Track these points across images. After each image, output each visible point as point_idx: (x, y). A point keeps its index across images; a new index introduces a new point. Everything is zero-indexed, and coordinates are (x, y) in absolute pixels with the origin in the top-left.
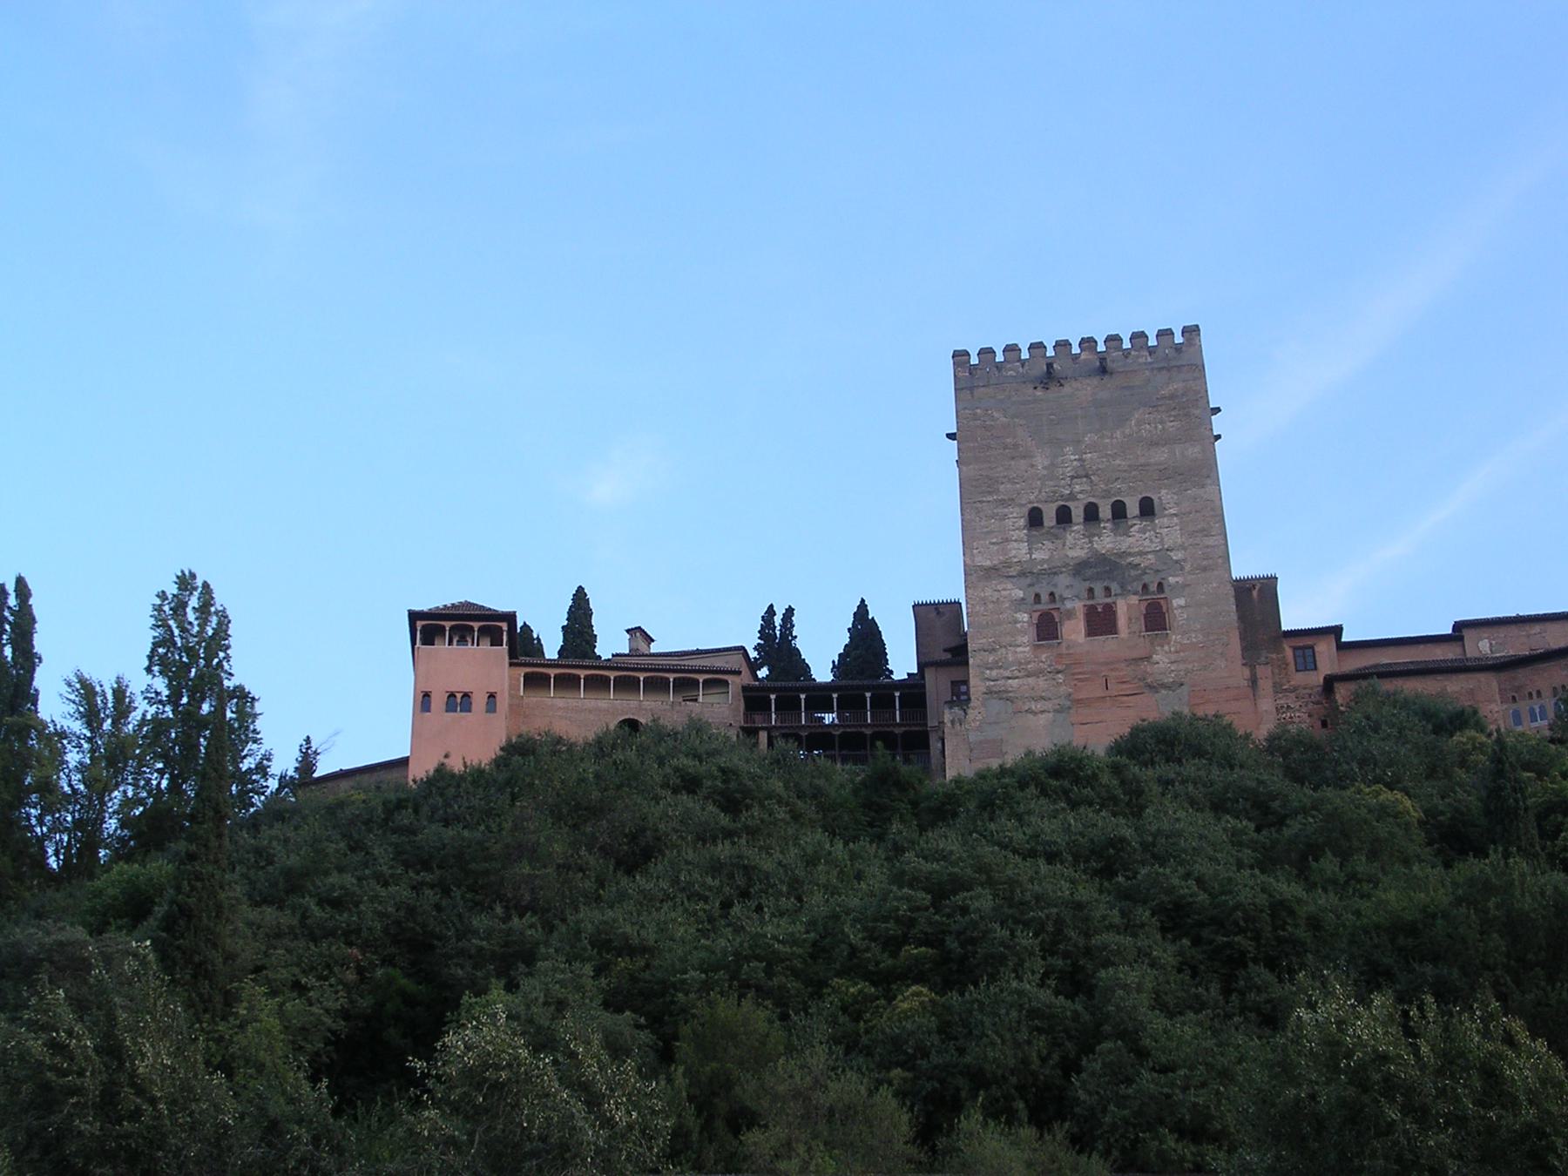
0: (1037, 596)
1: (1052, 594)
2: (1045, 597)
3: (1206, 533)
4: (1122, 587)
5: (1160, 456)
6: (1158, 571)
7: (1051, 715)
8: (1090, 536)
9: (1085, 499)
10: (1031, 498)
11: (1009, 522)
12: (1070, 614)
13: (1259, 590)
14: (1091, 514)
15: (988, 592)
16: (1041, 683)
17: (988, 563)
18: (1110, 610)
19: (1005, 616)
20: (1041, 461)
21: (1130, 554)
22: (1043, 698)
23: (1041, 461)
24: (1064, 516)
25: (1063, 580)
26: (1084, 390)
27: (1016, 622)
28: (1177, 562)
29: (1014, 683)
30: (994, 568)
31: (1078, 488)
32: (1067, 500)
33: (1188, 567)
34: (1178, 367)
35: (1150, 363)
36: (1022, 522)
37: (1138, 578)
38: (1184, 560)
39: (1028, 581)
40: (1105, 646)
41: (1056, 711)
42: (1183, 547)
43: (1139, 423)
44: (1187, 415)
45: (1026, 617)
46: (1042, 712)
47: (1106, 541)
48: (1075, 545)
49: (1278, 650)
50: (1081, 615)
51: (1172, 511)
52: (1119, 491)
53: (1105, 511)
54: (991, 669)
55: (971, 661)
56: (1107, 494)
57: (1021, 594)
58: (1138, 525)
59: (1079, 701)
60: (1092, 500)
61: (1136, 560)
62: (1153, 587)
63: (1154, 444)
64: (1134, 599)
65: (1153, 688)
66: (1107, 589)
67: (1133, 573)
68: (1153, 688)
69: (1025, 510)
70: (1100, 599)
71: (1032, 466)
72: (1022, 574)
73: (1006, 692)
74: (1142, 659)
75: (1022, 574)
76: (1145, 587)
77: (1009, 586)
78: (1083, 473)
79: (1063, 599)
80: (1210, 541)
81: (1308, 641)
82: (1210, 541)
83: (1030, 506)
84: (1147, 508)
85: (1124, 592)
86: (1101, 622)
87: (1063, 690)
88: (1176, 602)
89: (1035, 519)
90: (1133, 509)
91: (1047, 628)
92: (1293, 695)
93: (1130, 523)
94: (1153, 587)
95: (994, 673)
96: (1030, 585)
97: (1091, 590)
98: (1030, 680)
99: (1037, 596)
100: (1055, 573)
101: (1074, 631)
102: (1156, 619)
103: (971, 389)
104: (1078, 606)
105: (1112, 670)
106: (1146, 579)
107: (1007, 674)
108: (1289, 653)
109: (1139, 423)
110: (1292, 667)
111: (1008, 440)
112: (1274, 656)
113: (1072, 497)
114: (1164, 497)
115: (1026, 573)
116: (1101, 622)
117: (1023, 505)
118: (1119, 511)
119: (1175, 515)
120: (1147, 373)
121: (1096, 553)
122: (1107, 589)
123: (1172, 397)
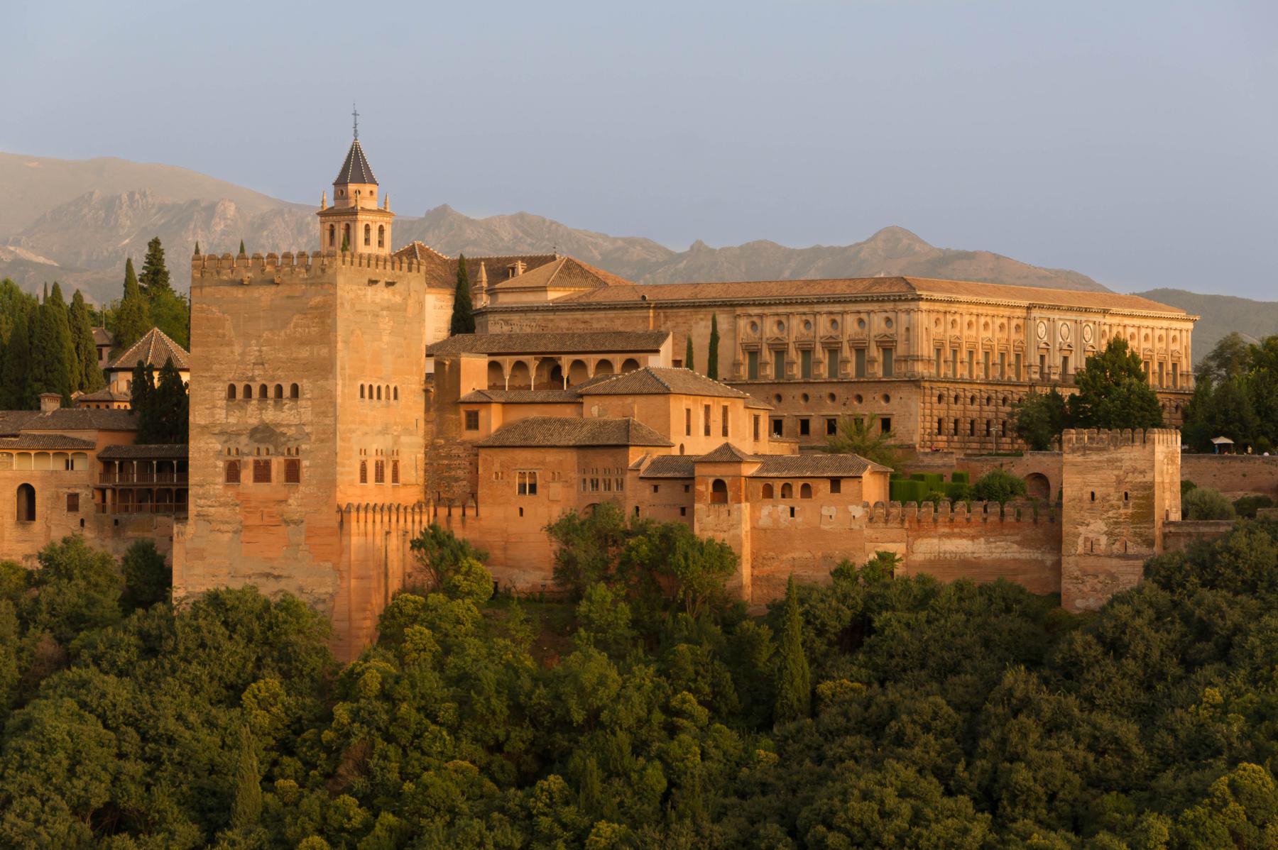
0: (229, 449)
1: (237, 449)
2: (233, 452)
3: (325, 414)
4: (276, 448)
5: (304, 353)
6: (296, 440)
7: (230, 535)
8: (261, 409)
9: (260, 381)
10: (229, 377)
11: (216, 393)
12: (246, 463)
13: (451, 365)
14: (264, 389)
15: (202, 444)
16: (227, 512)
17: (203, 423)
18: (267, 464)
19: (210, 461)
20: (237, 349)
21: (282, 425)
22: (227, 523)
23: (237, 349)
24: (248, 390)
25: (244, 440)
26: (265, 295)
27: (216, 467)
28: (307, 434)
29: (212, 510)
30: (206, 427)
31: (257, 372)
32: (250, 381)
33: (313, 438)
34: (322, 284)
35: (306, 279)
36: (224, 394)
37: (284, 444)
38: (311, 433)
39: (224, 438)
40: (263, 488)
41: (235, 532)
42: (312, 424)
43: (295, 328)
44: (323, 323)
45: (221, 464)
46: (227, 532)
47: (270, 415)
48: (253, 415)
49: (458, 413)
50: (251, 467)
51: (308, 396)
52: (279, 378)
53: (271, 392)
54: (200, 499)
55: (190, 492)
56: (273, 378)
57: (219, 447)
58: (288, 404)
59: (246, 527)
60: (264, 382)
61: (284, 430)
62: (293, 451)
63: (302, 343)
64: (281, 459)
65: (287, 522)
66: (268, 449)
67: (283, 439)
68: (287, 522)
69: (226, 386)
70: (264, 457)
71: (232, 352)
72: (222, 433)
73: (208, 516)
74: (282, 501)
75: (222, 433)
76: (289, 449)
77: (214, 441)
78: (260, 361)
79: (243, 454)
80: (327, 421)
81: (474, 408)
82: (327, 421)
83: (229, 383)
84: (295, 391)
85: (278, 453)
86: (262, 473)
87: (239, 517)
88: (305, 463)
89: (232, 390)
90: (287, 392)
91: (233, 473)
92: (462, 448)
93: (285, 401)
94: (293, 451)
95: (202, 502)
96: (226, 442)
97: (258, 449)
98: (221, 509)
99: (229, 449)
100: (239, 435)
101: (247, 475)
102: (293, 472)
103: (201, 288)
104: (250, 459)
105: (266, 507)
106: (290, 444)
107: (209, 503)
108: (463, 415)
109: (296, 326)
110: (464, 426)
111: (220, 331)
112: (453, 416)
113: (252, 379)
114: (305, 385)
115: (227, 434)
116: (262, 473)
117: (224, 382)
118: (279, 389)
119: (309, 399)
120: (304, 287)
121: (262, 422)
122: (268, 449)
123: (316, 308)
